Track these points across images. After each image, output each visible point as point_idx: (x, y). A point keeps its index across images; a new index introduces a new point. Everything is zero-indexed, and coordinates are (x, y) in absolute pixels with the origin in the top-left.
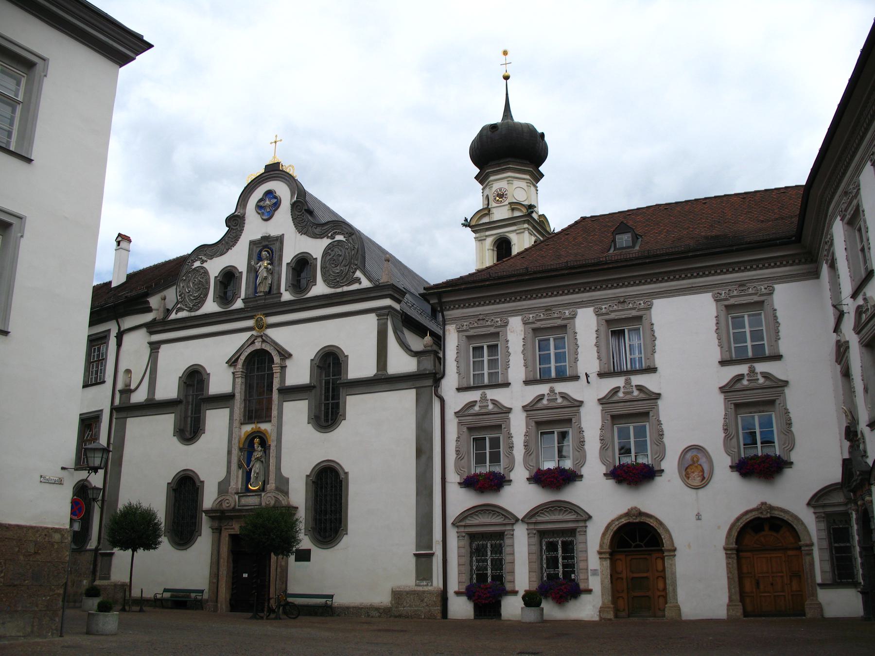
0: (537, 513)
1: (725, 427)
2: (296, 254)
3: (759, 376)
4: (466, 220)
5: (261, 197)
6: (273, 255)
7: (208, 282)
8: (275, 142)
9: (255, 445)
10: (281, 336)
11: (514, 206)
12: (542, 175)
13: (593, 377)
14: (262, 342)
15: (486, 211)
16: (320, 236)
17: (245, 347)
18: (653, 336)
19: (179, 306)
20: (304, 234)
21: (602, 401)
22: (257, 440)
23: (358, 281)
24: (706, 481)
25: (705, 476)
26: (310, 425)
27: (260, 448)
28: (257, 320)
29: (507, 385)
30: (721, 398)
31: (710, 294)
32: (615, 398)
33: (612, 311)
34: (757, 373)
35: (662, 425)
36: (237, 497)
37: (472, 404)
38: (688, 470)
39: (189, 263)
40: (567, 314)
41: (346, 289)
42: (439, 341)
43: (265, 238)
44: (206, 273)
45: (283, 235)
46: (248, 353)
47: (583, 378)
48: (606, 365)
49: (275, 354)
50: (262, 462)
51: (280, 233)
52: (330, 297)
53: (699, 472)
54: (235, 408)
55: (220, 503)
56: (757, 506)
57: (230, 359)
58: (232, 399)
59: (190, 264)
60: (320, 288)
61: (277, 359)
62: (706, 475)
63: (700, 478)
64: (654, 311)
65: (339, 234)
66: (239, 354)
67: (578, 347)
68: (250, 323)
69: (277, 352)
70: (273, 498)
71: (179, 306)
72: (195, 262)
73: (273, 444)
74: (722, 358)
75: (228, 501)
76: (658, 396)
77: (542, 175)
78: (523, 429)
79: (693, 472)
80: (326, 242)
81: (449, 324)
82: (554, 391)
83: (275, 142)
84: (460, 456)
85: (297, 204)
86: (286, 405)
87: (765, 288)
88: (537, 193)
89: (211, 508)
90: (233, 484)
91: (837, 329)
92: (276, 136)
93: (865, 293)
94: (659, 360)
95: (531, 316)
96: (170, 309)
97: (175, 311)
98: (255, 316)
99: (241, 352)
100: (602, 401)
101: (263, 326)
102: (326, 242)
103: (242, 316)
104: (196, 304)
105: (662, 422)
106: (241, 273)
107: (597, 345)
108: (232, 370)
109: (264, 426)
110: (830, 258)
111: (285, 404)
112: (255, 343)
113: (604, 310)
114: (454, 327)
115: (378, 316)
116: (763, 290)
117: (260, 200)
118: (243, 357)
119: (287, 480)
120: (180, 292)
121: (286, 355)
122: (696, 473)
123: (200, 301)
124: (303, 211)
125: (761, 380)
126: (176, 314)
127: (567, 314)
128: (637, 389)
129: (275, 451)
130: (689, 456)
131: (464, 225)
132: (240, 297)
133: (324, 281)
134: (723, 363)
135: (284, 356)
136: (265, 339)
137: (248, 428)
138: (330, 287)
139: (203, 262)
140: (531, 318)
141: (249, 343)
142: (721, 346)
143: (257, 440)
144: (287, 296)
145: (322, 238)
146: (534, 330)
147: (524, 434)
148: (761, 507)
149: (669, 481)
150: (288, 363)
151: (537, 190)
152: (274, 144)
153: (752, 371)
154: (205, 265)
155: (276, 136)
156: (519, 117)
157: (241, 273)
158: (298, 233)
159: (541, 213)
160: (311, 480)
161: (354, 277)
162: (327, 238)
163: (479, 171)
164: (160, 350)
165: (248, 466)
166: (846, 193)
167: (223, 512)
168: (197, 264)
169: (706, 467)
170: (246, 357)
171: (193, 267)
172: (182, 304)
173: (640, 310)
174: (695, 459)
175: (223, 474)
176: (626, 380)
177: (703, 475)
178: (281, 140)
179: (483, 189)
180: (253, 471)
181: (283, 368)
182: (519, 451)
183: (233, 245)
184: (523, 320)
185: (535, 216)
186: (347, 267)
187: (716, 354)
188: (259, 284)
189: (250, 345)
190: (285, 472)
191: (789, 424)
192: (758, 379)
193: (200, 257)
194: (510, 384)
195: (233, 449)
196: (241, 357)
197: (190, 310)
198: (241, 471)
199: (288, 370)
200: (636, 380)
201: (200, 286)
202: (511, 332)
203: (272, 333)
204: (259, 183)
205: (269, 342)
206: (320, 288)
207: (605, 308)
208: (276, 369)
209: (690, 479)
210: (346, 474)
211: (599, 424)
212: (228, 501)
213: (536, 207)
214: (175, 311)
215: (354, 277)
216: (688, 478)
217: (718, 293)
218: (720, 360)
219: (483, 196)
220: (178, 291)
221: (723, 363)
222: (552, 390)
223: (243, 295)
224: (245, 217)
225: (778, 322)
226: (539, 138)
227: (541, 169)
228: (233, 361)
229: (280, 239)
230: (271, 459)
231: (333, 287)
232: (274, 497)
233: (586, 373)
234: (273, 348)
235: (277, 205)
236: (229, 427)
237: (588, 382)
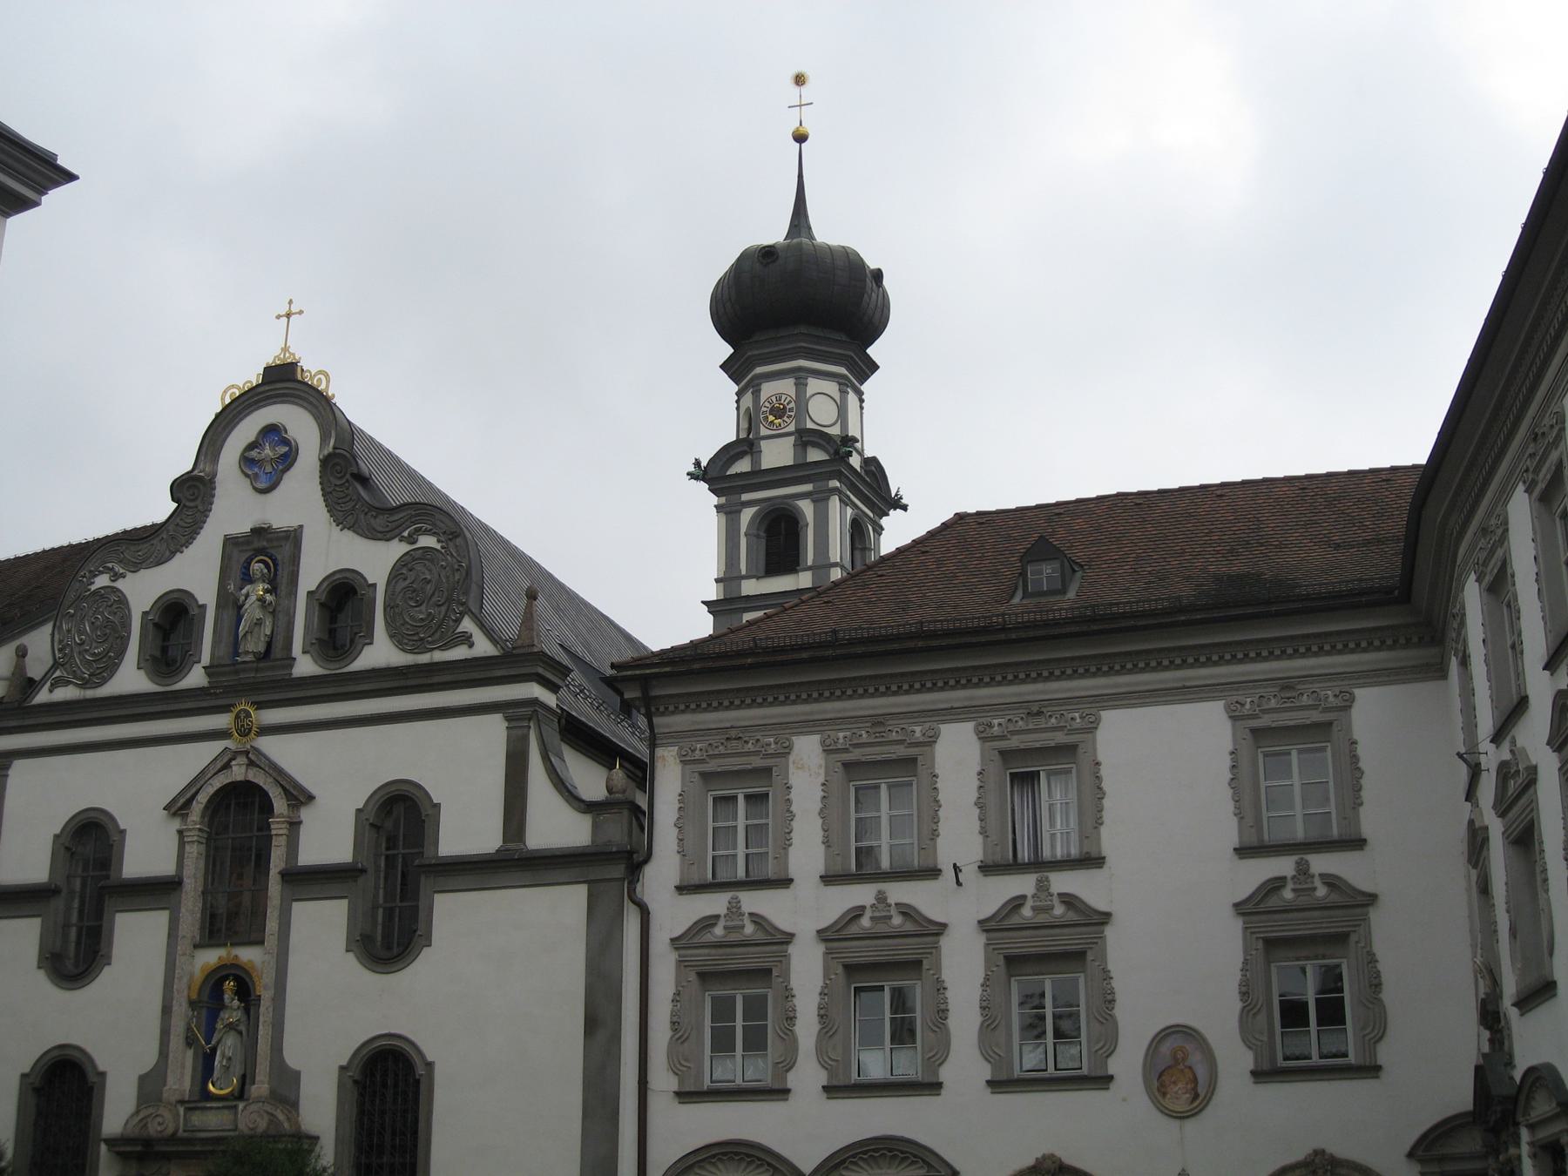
0: (843, 1162)
1: (1244, 989)
2: (327, 574)
3: (1318, 883)
4: (697, 463)
5: (252, 438)
6: (276, 570)
7: (126, 624)
8: (288, 316)
9: (226, 996)
10: (287, 753)
11: (807, 438)
12: (874, 367)
13: (970, 874)
14: (248, 765)
15: (744, 446)
16: (384, 536)
17: (210, 775)
18: (1100, 788)
19: (58, 673)
20: (349, 529)
21: (986, 926)
22: (229, 985)
23: (467, 640)
24: (1200, 1104)
25: (1200, 1090)
26: (351, 955)
27: (236, 1003)
28: (237, 717)
29: (785, 882)
30: (1237, 925)
31: (1221, 704)
32: (1015, 920)
33: (1013, 733)
34: (1313, 876)
35: (1111, 981)
36: (181, 1111)
37: (708, 922)
38: (1164, 1078)
39: (83, 577)
40: (918, 734)
41: (439, 656)
42: (641, 773)
43: (259, 532)
44: (122, 602)
45: (301, 526)
47: (949, 873)
48: (998, 848)
50: (240, 1033)
51: (295, 524)
52: (405, 674)
53: (1187, 1084)
54: (183, 910)
55: (144, 1121)
56: (1306, 1158)
57: (174, 800)
58: (175, 889)
59: (85, 579)
60: (380, 652)
61: (280, 805)
62: (1202, 1091)
63: (1188, 1095)
64: (1102, 735)
65: (427, 532)
66: (194, 790)
67: (940, 806)
68: (221, 721)
69: (280, 790)
70: (265, 1115)
71: (58, 673)
72: (96, 576)
73: (266, 995)
74: (1240, 842)
75: (160, 1120)
76: (1105, 918)
77: (874, 367)
78: (817, 981)
79: (1175, 1083)
80: (395, 550)
81: (663, 745)
82: (886, 899)
83: (288, 316)
84: (680, 1034)
85: (337, 460)
86: (297, 907)
87: (1335, 696)
88: (862, 408)
89: (122, 1134)
90: (172, 1082)
91: (1470, 795)
92: (291, 302)
93: (1514, 738)
94: (1109, 841)
95: (841, 735)
96: (37, 678)
97: (48, 684)
98: (233, 705)
100: (985, 925)
101: (250, 730)
102: (395, 550)
103: (204, 704)
104: (98, 671)
105: (1112, 975)
106: (203, 607)
107: (980, 804)
108: (176, 824)
109: (248, 955)
110: (1460, 647)
111: (296, 906)
112: (231, 767)
113: (996, 728)
114: (675, 753)
115: (508, 719)
116: (1331, 699)
117: (252, 446)
118: (203, 798)
119: (296, 1076)
120: (60, 641)
121: (299, 797)
122: (1180, 1085)
123: (108, 666)
124: (348, 476)
125: (1321, 891)
126: (51, 691)
127: (918, 734)
128: (1063, 902)
129: (271, 1009)
130: (1166, 1048)
131: (692, 476)
132: (199, 662)
133: (392, 637)
134: (1244, 851)
135: (296, 798)
136: (255, 759)
137: (211, 957)
138: (404, 650)
139: (116, 576)
140: (841, 741)
141: (219, 766)
142: (1239, 814)
143: (229, 985)
144: (305, 666)
145: (388, 540)
146: (847, 766)
147: (818, 990)
148: (1313, 1160)
149: (1124, 1100)
150: (305, 814)
151: (862, 401)
152: (285, 319)
153: (1303, 870)
154: (120, 584)
155: (291, 302)
156: (827, 231)
157: (203, 607)
158: (334, 524)
159: (868, 453)
160: (350, 1076)
161: (458, 630)
162: (401, 541)
163: (733, 351)
164: (10, 772)
165: (208, 1042)
166: (1484, 531)
167: (148, 1142)
168: (102, 581)
169: (1201, 1072)
170: (211, 797)
171: (93, 588)
172: (65, 670)
173: (1072, 731)
174: (1180, 1055)
175: (150, 1059)
176: (1039, 881)
177: (1195, 1089)
178: (301, 312)
179: (739, 394)
180: (218, 1053)
181: (295, 825)
182: (807, 1028)
183: (187, 544)
184: (823, 743)
185: (855, 461)
186: (443, 609)
187: (1230, 835)
188: (245, 635)
190: (292, 1058)
191: (1376, 986)
192: (1315, 889)
193: (110, 565)
194: (791, 880)
195: (174, 1002)
197: (85, 684)
198: (190, 1053)
199: (304, 832)
200: (1062, 882)
201: (108, 631)
202: (798, 768)
203: (271, 746)
204: (250, 405)
205: (263, 766)
206: (380, 652)
207: (1000, 724)
208: (278, 828)
209: (1168, 1096)
210: (430, 1066)
211: (979, 974)
212: (160, 1120)
213: (858, 441)
214: (48, 684)
215: (458, 630)
216: (1164, 1094)
217: (1237, 702)
218: (1237, 847)
219: (738, 408)
220: (57, 637)
221: (1243, 852)
222: (881, 898)
223: (206, 658)
224: (215, 482)
225: (1359, 769)
226: (870, 282)
227: (872, 351)
228: (179, 804)
229: (293, 537)
230: (261, 1027)
231: (411, 652)
232: (268, 1113)
233: (955, 865)
234: (272, 780)
235: (289, 458)
236: (168, 954)
237: (959, 883)
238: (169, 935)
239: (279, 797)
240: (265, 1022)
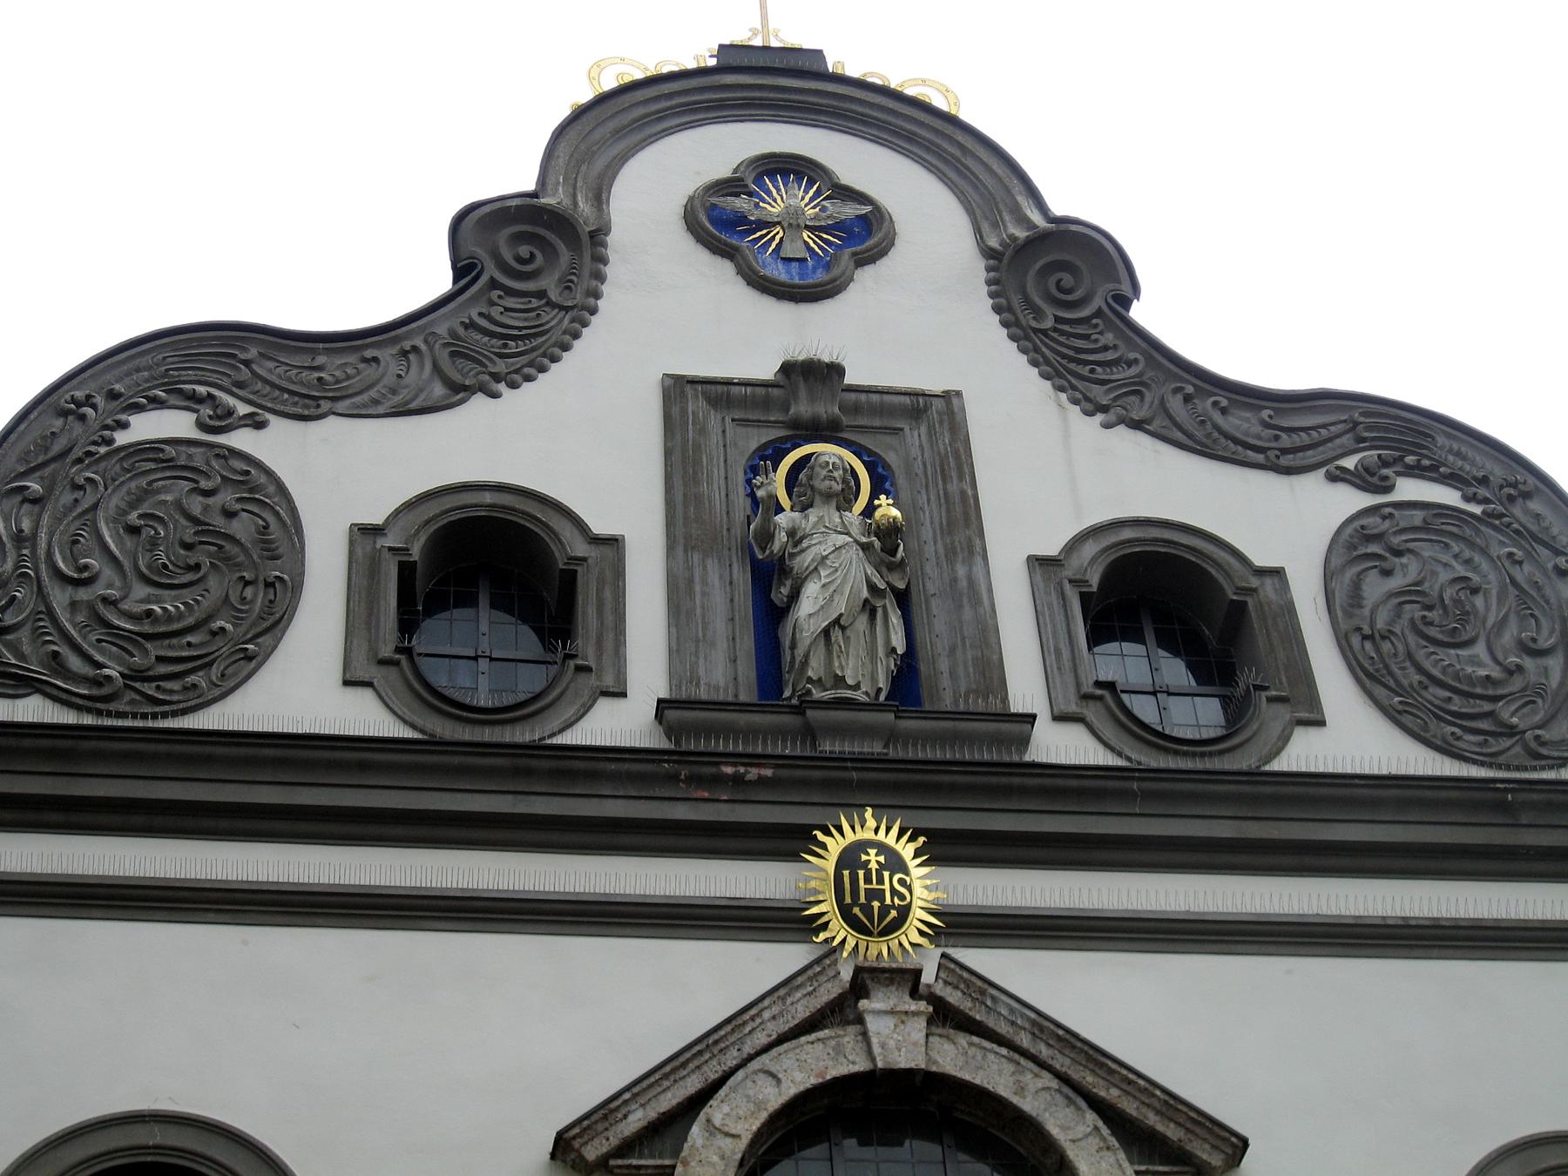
14: (930, 1021)
17: (761, 1039)
46: (791, 1090)
49: (1082, 1130)
57: (607, 1111)
66: (692, 1084)
69: (1091, 1117)
99: (712, 1074)
103: (681, 812)
104: (163, 669)
141: (802, 1009)
171: (122, 438)
189: (782, 1039)
196: (717, 1111)
205: (1003, 1028)
224: (604, 245)
239: (1094, 1142)
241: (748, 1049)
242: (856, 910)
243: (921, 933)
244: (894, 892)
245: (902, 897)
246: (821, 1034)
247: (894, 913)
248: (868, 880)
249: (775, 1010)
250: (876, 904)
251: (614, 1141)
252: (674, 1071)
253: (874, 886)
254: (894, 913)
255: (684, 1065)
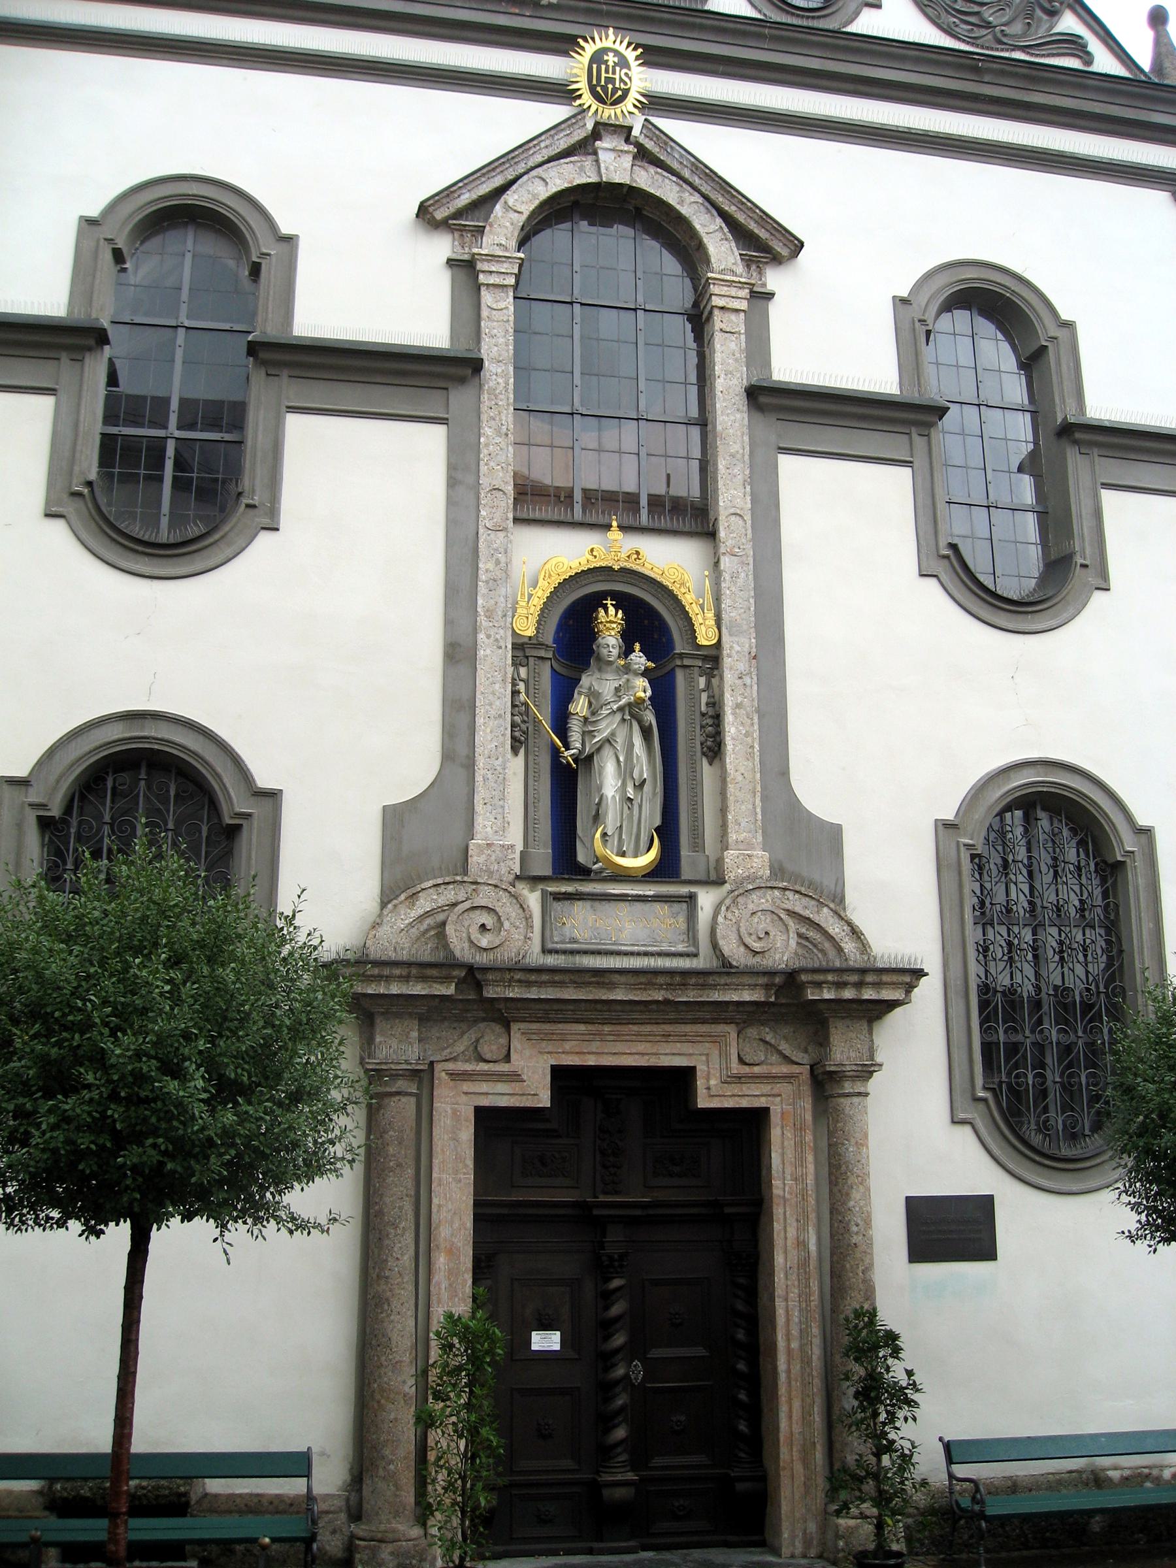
17: (539, 158)
22: (611, 620)
36: (533, 899)
46: (553, 189)
49: (713, 228)
54: (487, 431)
55: (441, 917)
57: (449, 192)
58: (462, 380)
66: (498, 181)
69: (719, 221)
70: (791, 923)
119: (833, 836)
135: (764, 248)
141: (563, 144)
143: (611, 620)
161: (1055, 30)
189: (550, 160)
195: (481, 636)
196: (510, 197)
199: (776, 311)
205: (675, 166)
236: (452, 524)
238: (452, 483)
239: (719, 235)
240: (738, 706)
241: (531, 164)
242: (599, 89)
243: (635, 106)
244: (621, 80)
245: (626, 84)
246: (572, 159)
247: (620, 93)
248: (607, 71)
249: (548, 142)
250: (610, 86)
251: (452, 210)
252: (489, 171)
253: (610, 75)
254: (620, 93)
255: (494, 170)
